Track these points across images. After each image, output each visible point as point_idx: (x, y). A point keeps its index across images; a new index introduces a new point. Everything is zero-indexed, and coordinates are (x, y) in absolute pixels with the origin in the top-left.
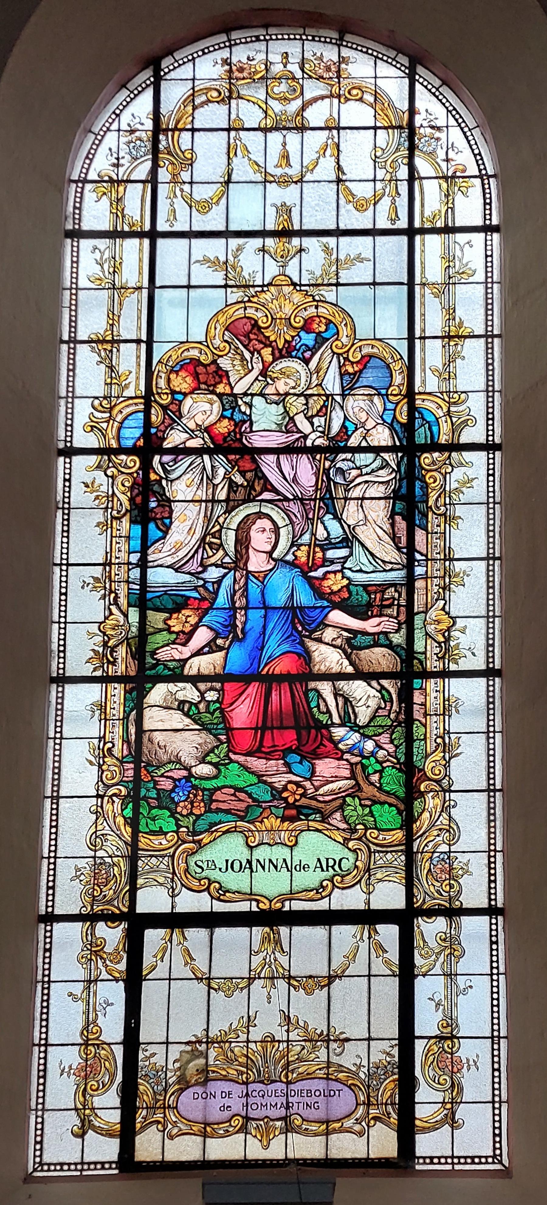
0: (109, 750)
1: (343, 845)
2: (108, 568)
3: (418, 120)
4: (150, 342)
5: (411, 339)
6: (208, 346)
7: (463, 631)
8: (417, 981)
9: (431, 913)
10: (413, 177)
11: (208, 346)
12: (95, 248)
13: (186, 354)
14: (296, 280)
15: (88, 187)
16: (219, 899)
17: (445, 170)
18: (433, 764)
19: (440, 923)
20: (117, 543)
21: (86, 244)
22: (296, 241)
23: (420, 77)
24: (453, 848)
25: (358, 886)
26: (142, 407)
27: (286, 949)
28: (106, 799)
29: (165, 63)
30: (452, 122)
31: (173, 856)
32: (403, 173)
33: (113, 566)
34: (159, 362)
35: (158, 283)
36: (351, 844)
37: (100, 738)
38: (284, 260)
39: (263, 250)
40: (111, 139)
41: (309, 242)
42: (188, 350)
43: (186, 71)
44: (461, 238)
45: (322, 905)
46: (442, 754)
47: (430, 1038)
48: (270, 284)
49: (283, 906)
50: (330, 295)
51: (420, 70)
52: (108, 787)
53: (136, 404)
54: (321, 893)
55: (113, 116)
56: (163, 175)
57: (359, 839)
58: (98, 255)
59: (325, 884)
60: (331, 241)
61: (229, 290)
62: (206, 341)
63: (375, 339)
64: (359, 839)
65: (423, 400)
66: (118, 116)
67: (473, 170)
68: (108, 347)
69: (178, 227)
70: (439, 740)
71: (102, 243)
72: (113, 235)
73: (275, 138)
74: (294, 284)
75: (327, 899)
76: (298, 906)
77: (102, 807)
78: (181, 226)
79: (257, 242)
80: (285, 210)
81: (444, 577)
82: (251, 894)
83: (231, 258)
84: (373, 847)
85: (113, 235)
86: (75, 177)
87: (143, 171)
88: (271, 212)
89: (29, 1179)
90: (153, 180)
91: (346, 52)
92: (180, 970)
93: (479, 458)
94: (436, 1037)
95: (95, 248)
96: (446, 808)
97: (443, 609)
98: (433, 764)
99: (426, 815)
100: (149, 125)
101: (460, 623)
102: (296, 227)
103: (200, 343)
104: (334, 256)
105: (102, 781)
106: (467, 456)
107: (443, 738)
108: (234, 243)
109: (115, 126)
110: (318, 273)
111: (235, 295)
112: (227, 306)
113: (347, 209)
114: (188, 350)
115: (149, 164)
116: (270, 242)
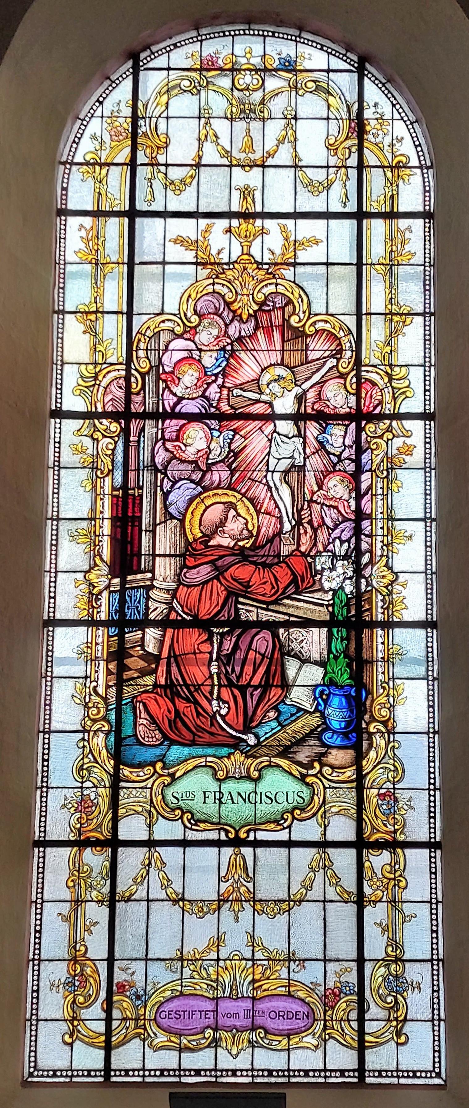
0: (95, 687)
1: (301, 780)
2: (93, 522)
3: (368, 114)
4: (130, 314)
5: (359, 315)
6: (181, 319)
7: (404, 586)
8: (365, 910)
9: (379, 846)
10: (361, 167)
11: (181, 319)
12: (81, 226)
13: (162, 325)
14: (259, 259)
15: (74, 168)
16: (191, 829)
17: (390, 160)
18: (379, 707)
19: (386, 856)
20: (101, 499)
21: (73, 222)
22: (259, 222)
23: (369, 72)
24: (396, 786)
25: (314, 818)
26: (123, 373)
27: (251, 875)
28: (92, 733)
29: (143, 56)
30: (397, 116)
31: (151, 788)
32: (353, 161)
33: (98, 521)
34: (138, 332)
35: (137, 260)
36: (308, 780)
37: (86, 677)
38: (248, 239)
39: (229, 230)
40: (95, 126)
41: (270, 224)
42: (163, 321)
43: (161, 62)
44: (403, 223)
45: (283, 836)
46: (386, 698)
47: (379, 961)
48: (236, 262)
49: (248, 836)
50: (288, 273)
51: (367, 65)
52: (95, 721)
53: (118, 370)
54: (282, 825)
55: (97, 104)
56: (141, 158)
57: (315, 776)
58: (83, 233)
59: (285, 817)
60: (290, 223)
61: (199, 268)
62: (179, 314)
63: (327, 314)
64: (315, 776)
65: (368, 372)
66: (101, 103)
67: (414, 162)
68: (93, 317)
69: (154, 208)
70: (384, 685)
71: (87, 221)
72: (97, 214)
73: (240, 126)
74: (256, 262)
75: (287, 830)
76: (261, 836)
77: (88, 742)
78: (157, 206)
79: (222, 224)
80: (247, 193)
81: (387, 536)
82: (219, 823)
83: (200, 238)
84: (327, 783)
85: (97, 214)
86: (64, 159)
87: (124, 155)
88: (236, 195)
89: (25, 1084)
90: (133, 164)
91: (302, 48)
92: (157, 893)
93: (417, 427)
94: (383, 960)
95: (81, 226)
96: (391, 746)
97: (386, 565)
98: (379, 707)
99: (372, 754)
100: (127, 112)
101: (402, 577)
102: (259, 209)
103: (175, 315)
104: (292, 238)
105: (88, 716)
106: (408, 424)
107: (388, 684)
108: (203, 222)
109: (98, 113)
110: (278, 251)
111: (203, 273)
112: (197, 281)
113: (303, 195)
114: (163, 321)
115: (128, 150)
116: (235, 222)
